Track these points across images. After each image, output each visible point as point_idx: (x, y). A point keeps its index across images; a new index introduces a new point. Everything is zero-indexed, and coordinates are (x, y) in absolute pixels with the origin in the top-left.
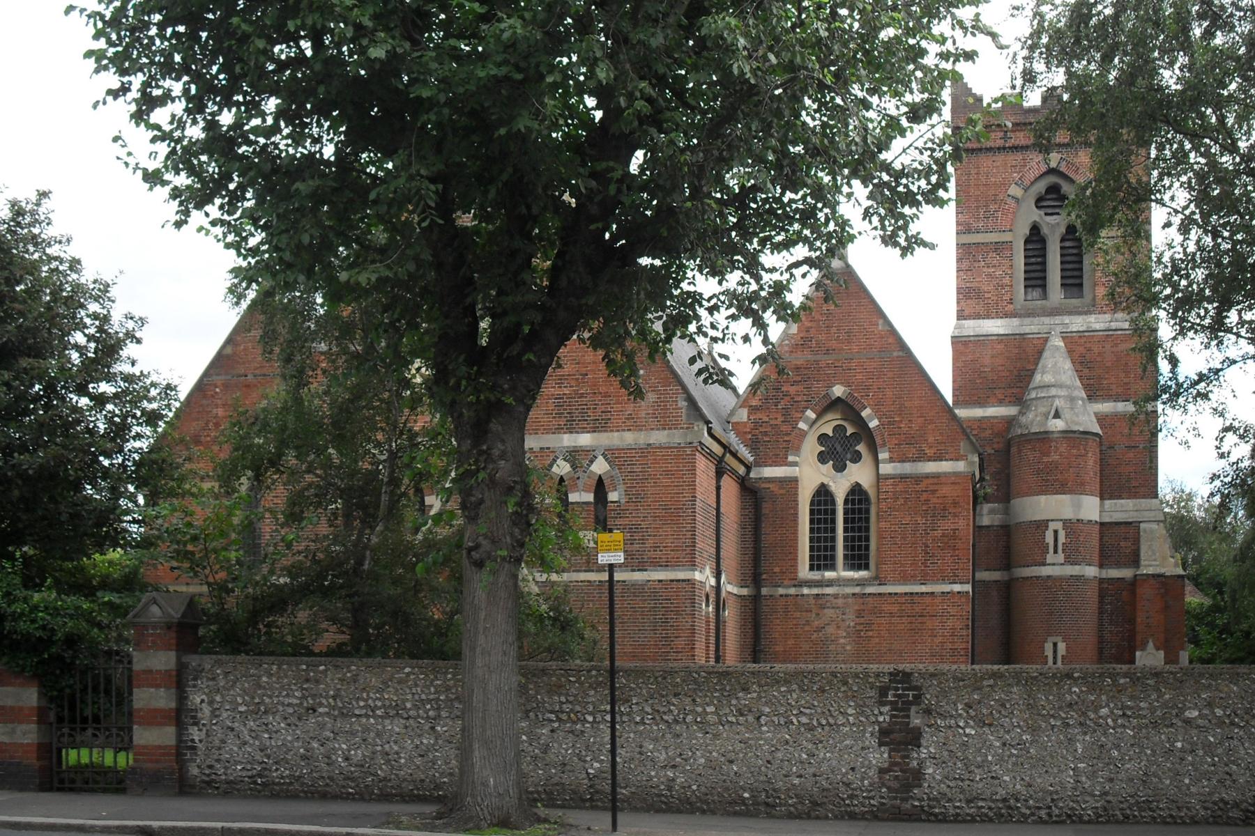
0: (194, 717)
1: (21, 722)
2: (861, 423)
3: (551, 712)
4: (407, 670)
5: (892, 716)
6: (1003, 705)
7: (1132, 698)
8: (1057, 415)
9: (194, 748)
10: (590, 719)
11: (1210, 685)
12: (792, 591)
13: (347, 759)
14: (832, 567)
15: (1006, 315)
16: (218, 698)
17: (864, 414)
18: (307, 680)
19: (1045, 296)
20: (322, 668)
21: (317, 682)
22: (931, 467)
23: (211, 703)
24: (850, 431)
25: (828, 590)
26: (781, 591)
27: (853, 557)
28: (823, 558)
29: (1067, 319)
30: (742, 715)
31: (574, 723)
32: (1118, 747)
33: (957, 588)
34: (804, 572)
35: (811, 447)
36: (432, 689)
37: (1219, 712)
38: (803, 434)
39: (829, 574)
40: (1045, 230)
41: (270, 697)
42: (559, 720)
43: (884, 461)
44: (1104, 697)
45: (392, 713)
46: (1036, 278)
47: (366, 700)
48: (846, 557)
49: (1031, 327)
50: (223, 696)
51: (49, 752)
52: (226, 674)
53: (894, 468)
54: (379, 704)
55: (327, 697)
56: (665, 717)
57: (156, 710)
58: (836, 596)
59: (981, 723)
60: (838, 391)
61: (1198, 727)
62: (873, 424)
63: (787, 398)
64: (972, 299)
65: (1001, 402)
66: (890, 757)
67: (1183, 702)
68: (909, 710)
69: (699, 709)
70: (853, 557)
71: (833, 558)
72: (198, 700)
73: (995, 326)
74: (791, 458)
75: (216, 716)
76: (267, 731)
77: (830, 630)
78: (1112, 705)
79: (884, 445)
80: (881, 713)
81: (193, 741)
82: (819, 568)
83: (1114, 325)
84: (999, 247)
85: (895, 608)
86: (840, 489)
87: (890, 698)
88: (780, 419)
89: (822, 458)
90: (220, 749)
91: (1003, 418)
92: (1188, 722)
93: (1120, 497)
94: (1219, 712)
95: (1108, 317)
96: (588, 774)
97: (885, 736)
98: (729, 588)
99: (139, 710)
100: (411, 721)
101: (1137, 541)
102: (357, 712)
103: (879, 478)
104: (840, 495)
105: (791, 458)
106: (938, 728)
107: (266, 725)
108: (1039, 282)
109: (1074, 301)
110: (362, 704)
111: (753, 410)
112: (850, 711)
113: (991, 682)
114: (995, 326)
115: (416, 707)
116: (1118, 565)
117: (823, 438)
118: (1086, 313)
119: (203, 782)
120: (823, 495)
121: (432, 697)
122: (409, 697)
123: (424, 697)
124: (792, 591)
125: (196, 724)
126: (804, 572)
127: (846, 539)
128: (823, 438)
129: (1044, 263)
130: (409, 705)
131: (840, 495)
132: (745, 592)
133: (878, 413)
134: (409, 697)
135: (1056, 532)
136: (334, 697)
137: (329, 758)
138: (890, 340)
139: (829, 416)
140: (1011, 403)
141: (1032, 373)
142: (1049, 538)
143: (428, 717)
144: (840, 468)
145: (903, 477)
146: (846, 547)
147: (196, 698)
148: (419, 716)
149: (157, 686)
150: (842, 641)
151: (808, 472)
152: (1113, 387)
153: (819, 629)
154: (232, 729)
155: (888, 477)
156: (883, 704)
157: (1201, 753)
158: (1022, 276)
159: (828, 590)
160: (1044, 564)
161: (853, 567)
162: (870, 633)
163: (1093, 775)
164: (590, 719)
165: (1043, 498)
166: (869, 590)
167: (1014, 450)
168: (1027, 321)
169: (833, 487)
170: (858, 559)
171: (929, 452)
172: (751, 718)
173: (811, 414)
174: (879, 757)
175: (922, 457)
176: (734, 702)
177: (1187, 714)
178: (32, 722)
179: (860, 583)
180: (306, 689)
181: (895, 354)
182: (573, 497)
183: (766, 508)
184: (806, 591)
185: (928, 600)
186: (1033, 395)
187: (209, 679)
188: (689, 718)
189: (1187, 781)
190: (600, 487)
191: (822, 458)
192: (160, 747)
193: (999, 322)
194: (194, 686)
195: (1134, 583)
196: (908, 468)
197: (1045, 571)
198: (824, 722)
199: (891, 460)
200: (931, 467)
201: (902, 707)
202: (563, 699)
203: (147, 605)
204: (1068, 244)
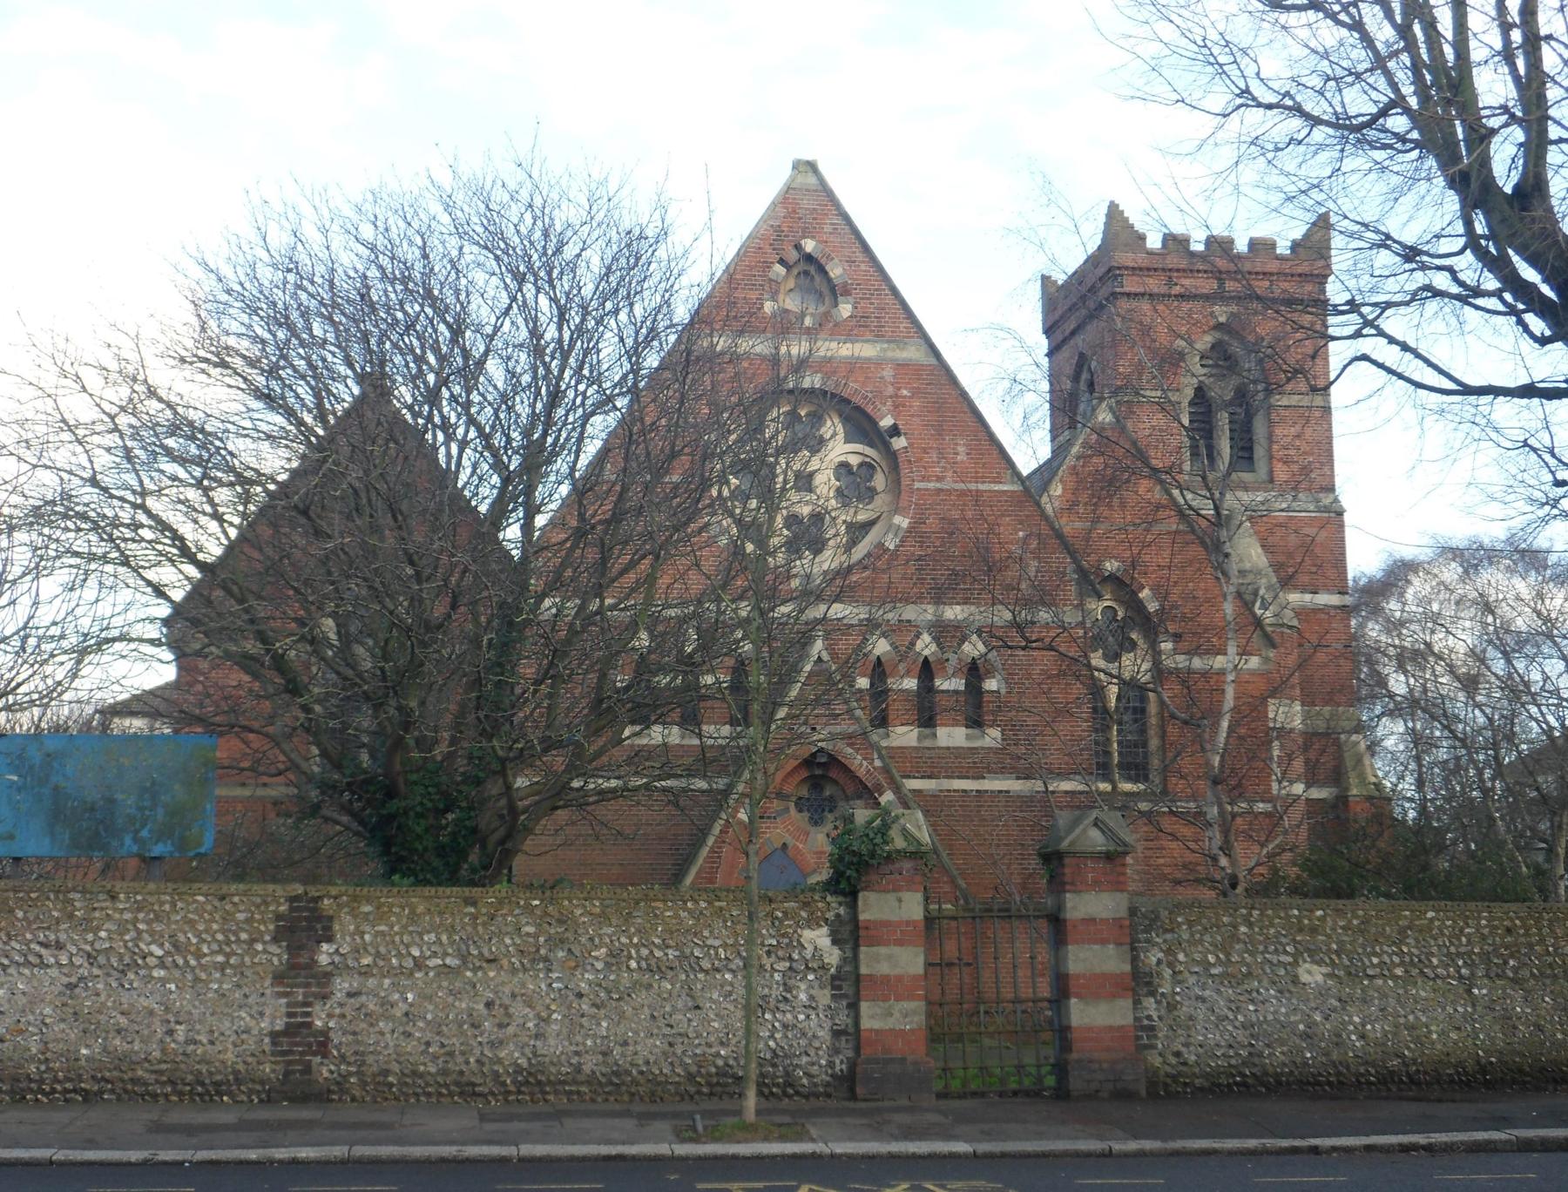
0: (1149, 984)
1: (897, 1000)
2: (1136, 606)
4: (1430, 914)
9: (1152, 1028)
13: (1362, 1037)
18: (1301, 930)
20: (1320, 913)
21: (1314, 931)
23: (1170, 965)
36: (1464, 939)
41: (1252, 954)
45: (1415, 972)
52: (1190, 924)
57: (1104, 976)
62: (1152, 607)
72: (1154, 960)
75: (1179, 982)
76: (1252, 1001)
81: (1149, 1018)
90: (1189, 1028)
99: (1078, 976)
102: (1370, 972)
107: (1249, 993)
119: (1167, 1075)
121: (1463, 950)
125: (1153, 994)
130: (1435, 961)
136: (1338, 953)
143: (1461, 977)
148: (1449, 976)
149: (1103, 942)
154: (1203, 1000)
178: (918, 998)
180: (1299, 943)
182: (943, 684)
187: (1166, 931)
190: (974, 672)
192: (1111, 1028)
194: (1148, 941)
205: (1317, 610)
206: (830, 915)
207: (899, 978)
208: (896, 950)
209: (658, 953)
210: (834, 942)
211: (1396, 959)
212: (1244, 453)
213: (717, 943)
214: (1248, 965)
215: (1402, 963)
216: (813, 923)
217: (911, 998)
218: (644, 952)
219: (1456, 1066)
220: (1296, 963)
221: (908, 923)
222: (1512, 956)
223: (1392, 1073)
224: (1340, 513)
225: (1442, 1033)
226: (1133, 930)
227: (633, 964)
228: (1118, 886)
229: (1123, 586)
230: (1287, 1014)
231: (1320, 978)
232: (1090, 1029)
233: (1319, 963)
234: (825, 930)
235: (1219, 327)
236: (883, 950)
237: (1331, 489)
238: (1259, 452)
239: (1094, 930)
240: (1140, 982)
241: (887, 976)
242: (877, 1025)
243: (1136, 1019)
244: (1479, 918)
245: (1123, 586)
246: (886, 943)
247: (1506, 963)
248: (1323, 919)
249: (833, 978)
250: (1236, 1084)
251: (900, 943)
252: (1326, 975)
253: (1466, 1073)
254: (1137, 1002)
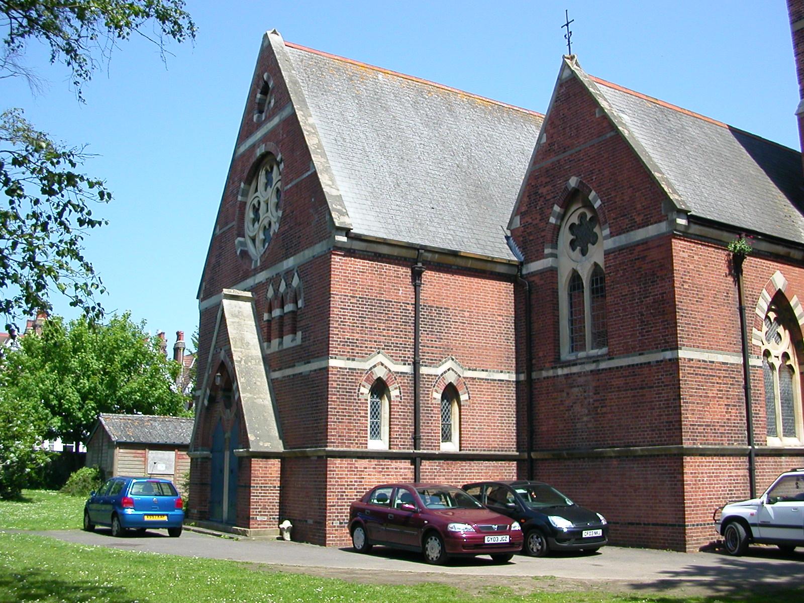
24: (589, 215)
25: (575, 369)
26: (545, 374)
35: (566, 236)
39: (582, 354)
53: (614, 242)
58: (579, 374)
62: (597, 204)
63: (542, 199)
77: (577, 408)
79: (606, 222)
88: (539, 217)
104: (585, 275)
117: (572, 227)
120: (575, 280)
126: (566, 354)
131: (585, 275)
133: (600, 195)
138: (605, 125)
150: (585, 419)
153: (569, 408)
159: (575, 369)
161: (599, 346)
162: (604, 410)
166: (603, 365)
170: (601, 339)
171: (638, 219)
173: (557, 208)
181: (608, 135)
191: (573, 245)
196: (622, 240)
199: (612, 235)
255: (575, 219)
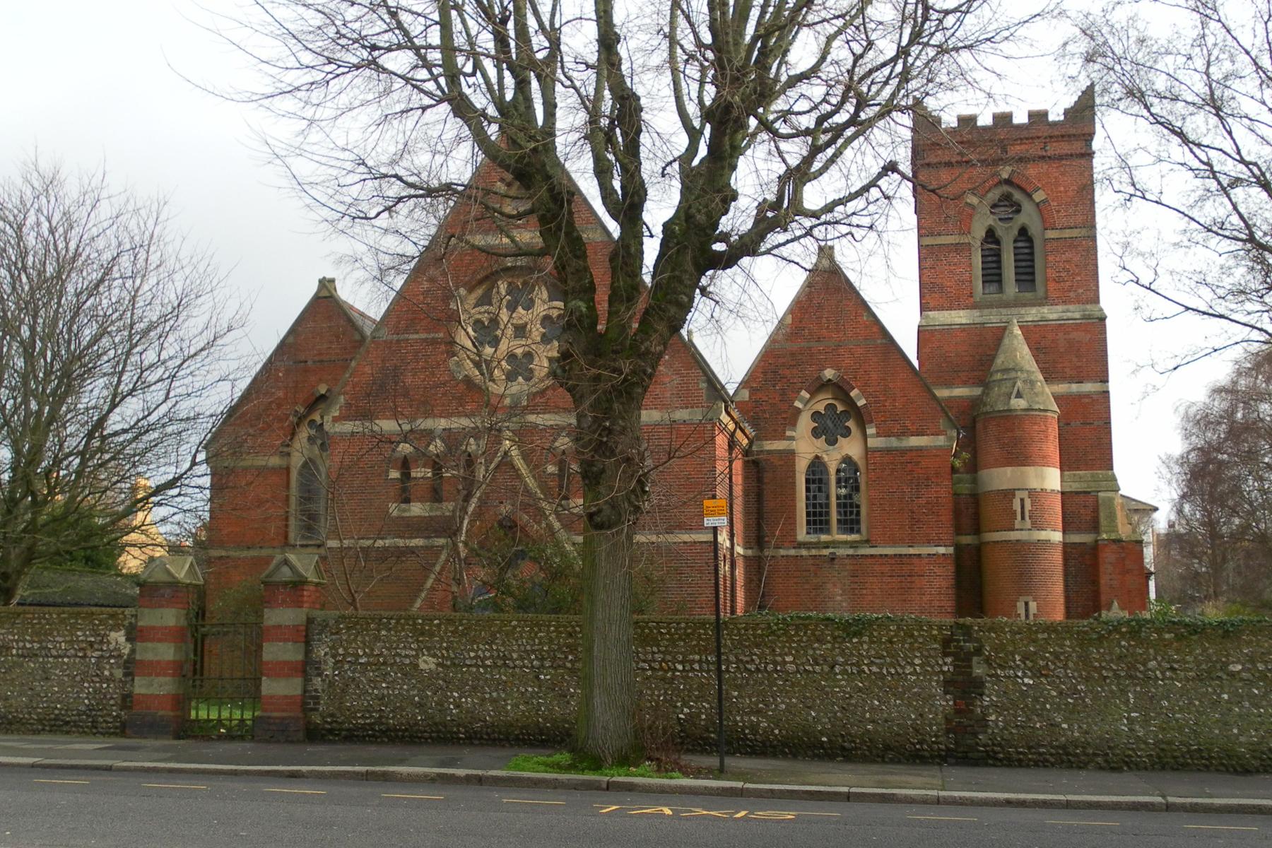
2: (851, 403)
3: (644, 661)
4: (514, 623)
5: (955, 667)
6: (1057, 657)
7: (1178, 651)
8: (1019, 395)
9: (317, 698)
10: (680, 667)
11: (1251, 641)
12: (792, 552)
13: (457, 706)
14: (828, 532)
15: (967, 308)
16: (341, 651)
17: (852, 394)
18: (422, 634)
19: (1001, 290)
21: (432, 635)
22: (915, 441)
23: (334, 656)
24: (840, 408)
26: (782, 552)
27: (845, 522)
28: (818, 520)
29: (1023, 311)
30: (817, 664)
31: (666, 672)
32: (1168, 698)
33: (942, 550)
34: (802, 534)
35: (805, 423)
37: (1261, 667)
38: (799, 411)
39: (824, 537)
40: (999, 233)
41: (388, 649)
42: (652, 668)
43: (872, 436)
44: (1151, 651)
45: (500, 663)
46: (993, 275)
47: (476, 652)
48: (839, 521)
49: (993, 318)
50: (345, 649)
51: (180, 702)
52: (348, 629)
54: (488, 654)
55: (441, 648)
56: (749, 666)
57: (285, 663)
59: (1037, 673)
60: (829, 373)
61: (1242, 680)
64: (933, 292)
65: (965, 383)
66: (955, 704)
67: (1226, 656)
68: (970, 660)
69: (779, 659)
70: (845, 522)
71: (828, 522)
73: (960, 317)
74: (788, 433)
78: (1159, 658)
79: (871, 422)
80: (945, 664)
81: (316, 690)
82: (815, 531)
83: (1066, 315)
84: (958, 248)
85: (886, 569)
86: (832, 460)
87: (953, 650)
89: (816, 433)
91: (968, 398)
92: (1232, 675)
93: (1078, 469)
94: (1261, 667)
95: (1060, 308)
96: (679, 719)
97: (948, 684)
98: (739, 550)
99: (267, 663)
100: (517, 670)
101: (1096, 510)
102: (468, 662)
103: (867, 450)
105: (788, 433)
106: (997, 676)
108: (995, 278)
109: (1029, 295)
110: (472, 654)
111: (753, 391)
112: (917, 661)
113: (1046, 635)
114: (960, 317)
115: (522, 658)
116: (1079, 530)
118: (1041, 305)
120: (817, 465)
122: (515, 648)
123: (528, 648)
124: (792, 552)
125: (320, 675)
126: (802, 534)
127: (839, 505)
128: (816, 416)
129: (999, 262)
130: (515, 656)
132: (750, 552)
133: (864, 393)
134: (515, 648)
135: (1022, 500)
136: (447, 649)
137: (442, 705)
138: (875, 330)
139: (821, 397)
140: (974, 384)
141: (992, 358)
142: (1017, 505)
143: (533, 667)
144: (832, 442)
145: (888, 451)
146: (839, 513)
147: (321, 651)
149: (286, 640)
151: (804, 445)
152: (1067, 370)
154: (354, 679)
155: (876, 450)
156: (946, 655)
157: (1247, 704)
158: (980, 273)
160: (1013, 530)
161: (845, 531)
163: (1146, 722)
164: (680, 667)
165: (1009, 470)
167: (979, 426)
168: (986, 311)
169: (826, 458)
170: (850, 522)
172: (826, 668)
174: (944, 703)
175: (905, 433)
176: (811, 652)
177: (1231, 667)
179: (853, 545)
183: (767, 476)
184: (804, 552)
185: (915, 561)
186: (999, 376)
187: (332, 634)
188: (770, 667)
189: (1235, 731)
191: (816, 433)
192: (286, 697)
193: (962, 313)
195: (1095, 548)
196: (894, 442)
197: (1013, 536)
198: (893, 671)
199: (878, 435)
200: (915, 441)
201: (963, 660)
202: (655, 649)
203: (278, 567)
204: (1020, 244)
205: (1080, 396)
206: (126, 623)
207: (158, 662)
208: (159, 645)
209: (28, 645)
210: (127, 640)
211: (488, 654)
212: (1026, 276)
213: (60, 639)
214: (385, 657)
215: (492, 657)
216: (116, 628)
217: (165, 675)
218: (21, 644)
219: (522, 728)
220: (417, 657)
221: (166, 628)
222: (571, 652)
223: (475, 733)
224: (1103, 319)
225: (516, 706)
226: (306, 635)
227: (14, 652)
228: (299, 604)
229: (840, 389)
230: (407, 691)
231: (433, 666)
232: (272, 697)
233: (434, 656)
234: (123, 632)
235: (1008, 182)
236: (149, 645)
237: (1096, 300)
238: (1039, 277)
239: (280, 633)
240: (307, 667)
241: (151, 662)
242: (143, 691)
243: (305, 691)
244: (549, 626)
245: (840, 389)
246: (152, 640)
247: (566, 658)
248: (439, 626)
249: (126, 662)
250: (369, 736)
251: (160, 640)
252: (438, 665)
253: (529, 735)
254: (307, 680)
255: (821, 407)
